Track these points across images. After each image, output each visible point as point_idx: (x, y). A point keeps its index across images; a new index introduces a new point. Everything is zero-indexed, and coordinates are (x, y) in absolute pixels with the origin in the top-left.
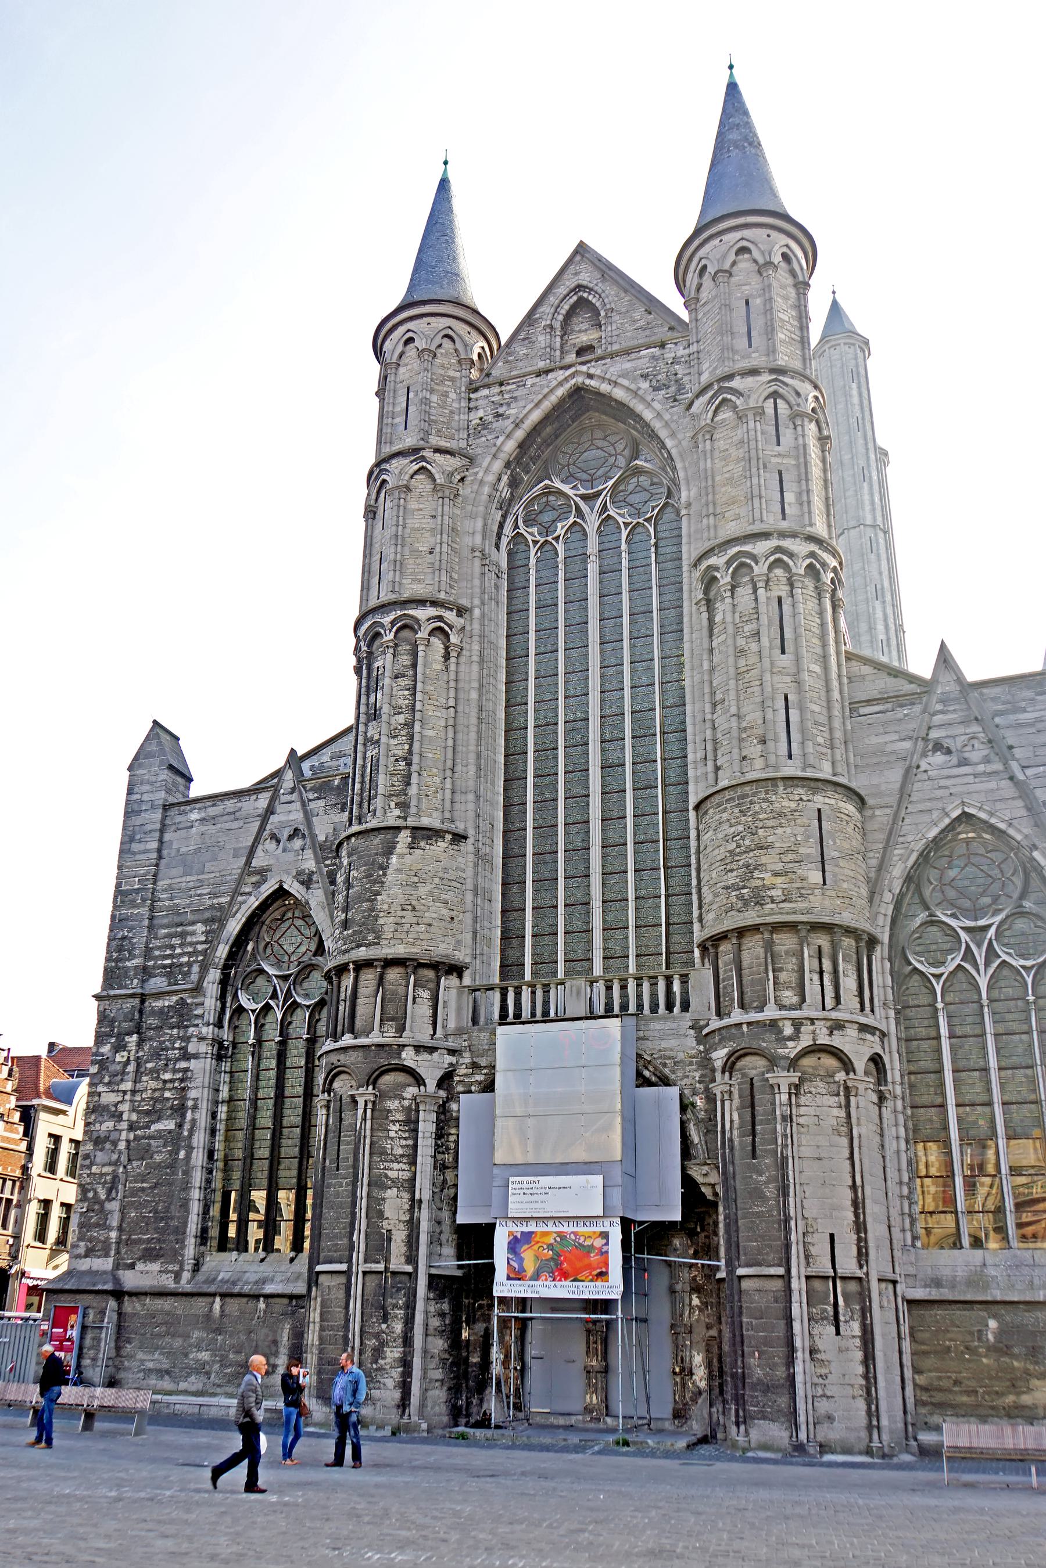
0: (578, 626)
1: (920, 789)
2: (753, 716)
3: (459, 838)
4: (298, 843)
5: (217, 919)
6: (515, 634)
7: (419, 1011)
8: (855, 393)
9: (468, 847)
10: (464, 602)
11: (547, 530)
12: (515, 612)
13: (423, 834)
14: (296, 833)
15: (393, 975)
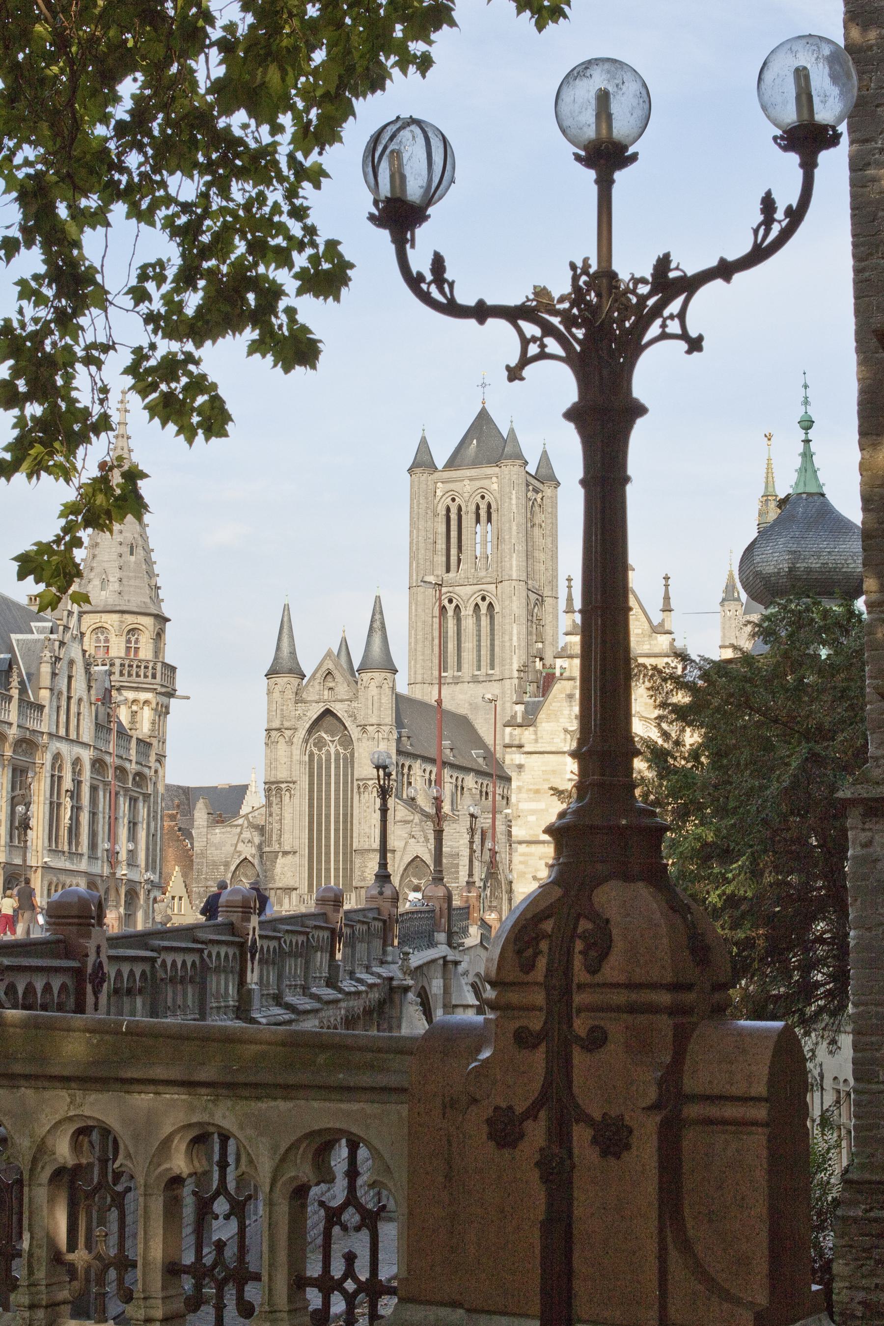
0: (328, 784)
1: (409, 848)
2: (367, 830)
3: (295, 853)
4: (250, 845)
5: (227, 865)
6: (311, 784)
7: (286, 901)
8: (514, 497)
9: (297, 854)
10: (294, 779)
11: (320, 750)
12: (311, 776)
13: (286, 853)
14: (249, 841)
15: (278, 891)
